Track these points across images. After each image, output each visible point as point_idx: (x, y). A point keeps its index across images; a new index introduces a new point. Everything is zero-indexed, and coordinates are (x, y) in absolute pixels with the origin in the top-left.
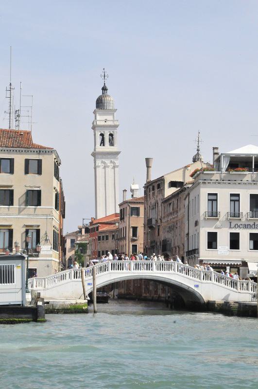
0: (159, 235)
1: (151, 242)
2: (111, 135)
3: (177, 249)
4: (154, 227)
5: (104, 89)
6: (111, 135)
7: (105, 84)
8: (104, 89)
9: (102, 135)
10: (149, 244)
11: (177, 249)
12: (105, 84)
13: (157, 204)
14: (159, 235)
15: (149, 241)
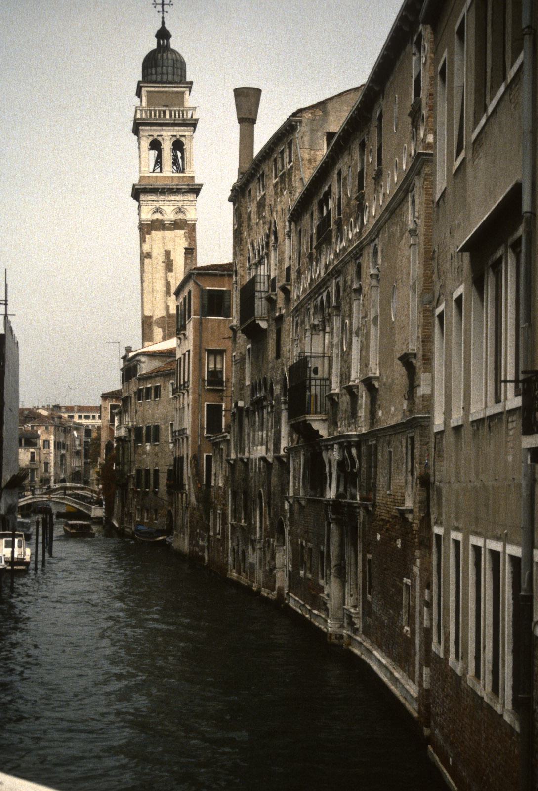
0: (278, 356)
1: (254, 388)
2: (178, 146)
3: (363, 399)
4: (264, 325)
5: (163, 34)
6: (178, 146)
7: (163, 23)
8: (163, 34)
9: (155, 145)
10: (248, 392)
11: (363, 399)
12: (163, 23)
13: (273, 238)
14: (278, 356)
15: (248, 383)
